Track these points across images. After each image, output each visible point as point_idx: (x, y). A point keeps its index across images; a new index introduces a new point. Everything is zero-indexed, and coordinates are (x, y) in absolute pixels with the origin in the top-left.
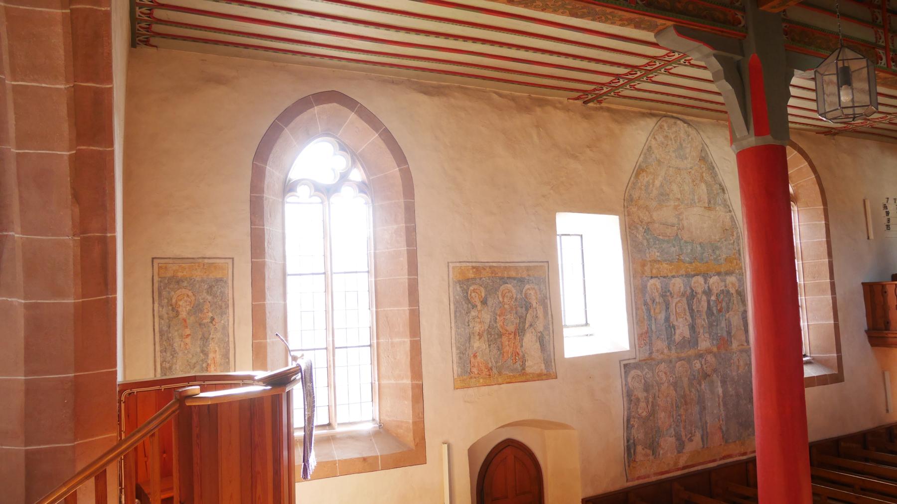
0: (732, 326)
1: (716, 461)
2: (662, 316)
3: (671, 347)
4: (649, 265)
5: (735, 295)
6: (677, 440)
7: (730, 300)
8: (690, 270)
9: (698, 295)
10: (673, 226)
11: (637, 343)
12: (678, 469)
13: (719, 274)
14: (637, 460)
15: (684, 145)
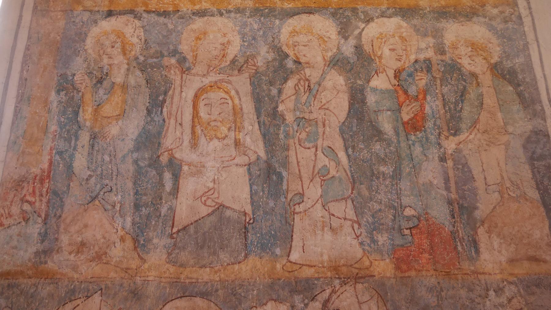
0: (480, 184)
3: (149, 240)
5: (486, 79)
7: (463, 94)
9: (308, 72)
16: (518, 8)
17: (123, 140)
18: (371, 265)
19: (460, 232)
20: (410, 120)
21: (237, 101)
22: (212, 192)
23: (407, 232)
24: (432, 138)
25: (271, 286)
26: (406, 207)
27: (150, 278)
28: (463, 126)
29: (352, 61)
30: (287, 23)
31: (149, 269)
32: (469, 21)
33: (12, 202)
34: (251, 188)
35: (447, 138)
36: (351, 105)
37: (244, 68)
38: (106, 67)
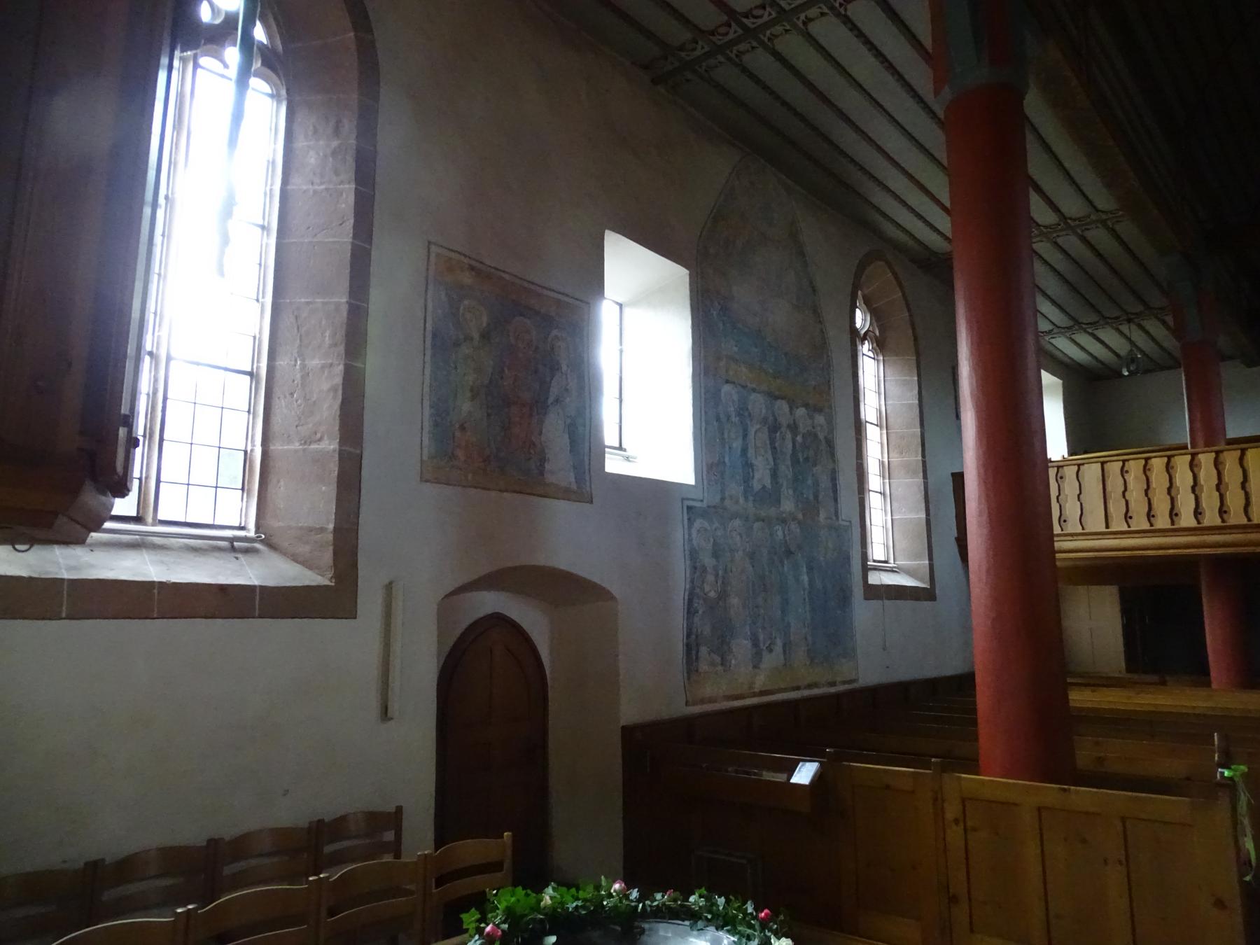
2: (737, 445)
5: (823, 442)
11: (705, 477)
12: (754, 695)
13: (806, 406)
14: (700, 670)
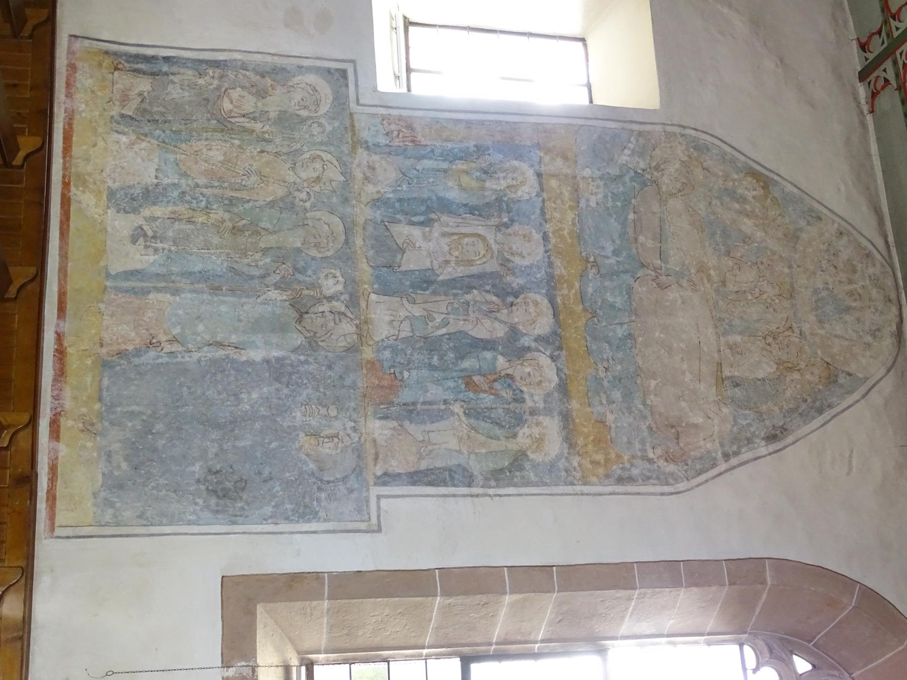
0: (429, 427)
1: (59, 317)
3: (379, 208)
4: (566, 171)
5: (512, 446)
6: (147, 192)
8: (565, 292)
9: (505, 311)
10: (662, 255)
12: (66, 185)
13: (564, 388)
14: (116, 73)
15: (848, 318)
16: (581, 485)
17: (444, 190)
18: (369, 345)
19: (394, 408)
20: (474, 381)
21: (478, 262)
22: (413, 246)
23: (392, 371)
24: (461, 396)
25: (354, 281)
26: (409, 372)
27: (355, 209)
28: (472, 421)
29: (516, 343)
30: (543, 298)
31: (361, 209)
32: (563, 439)
33: (398, 124)
34: (417, 270)
35: (462, 407)
36: (482, 340)
37: (504, 267)
38: (497, 176)
